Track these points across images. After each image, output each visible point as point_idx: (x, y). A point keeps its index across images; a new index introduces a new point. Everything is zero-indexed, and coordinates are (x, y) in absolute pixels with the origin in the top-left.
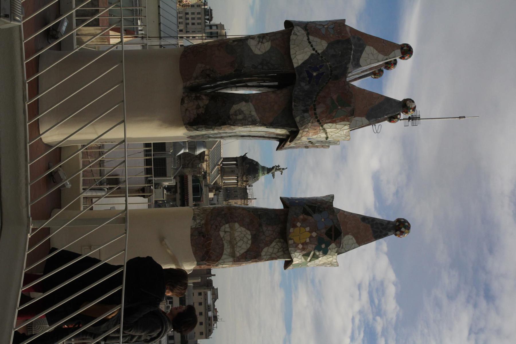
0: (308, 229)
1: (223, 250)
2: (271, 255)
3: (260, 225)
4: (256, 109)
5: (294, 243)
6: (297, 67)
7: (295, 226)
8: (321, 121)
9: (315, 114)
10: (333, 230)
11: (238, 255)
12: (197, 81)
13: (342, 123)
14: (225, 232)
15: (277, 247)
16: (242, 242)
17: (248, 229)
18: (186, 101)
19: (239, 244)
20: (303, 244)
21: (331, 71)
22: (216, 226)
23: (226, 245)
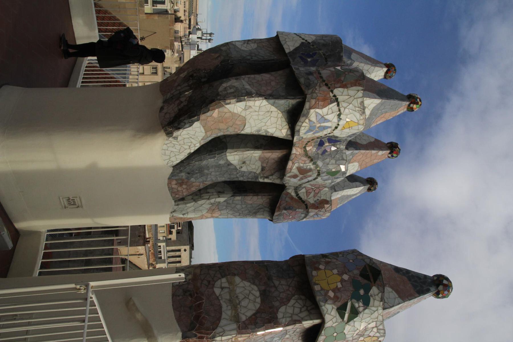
0: (335, 271)
1: (221, 313)
2: (291, 317)
3: (270, 278)
4: (250, 85)
5: (322, 289)
6: (289, 53)
7: (318, 269)
8: (329, 85)
9: (321, 77)
10: (368, 270)
11: (244, 318)
12: (179, 88)
13: (354, 88)
14: (222, 288)
15: (297, 305)
16: (247, 301)
17: (254, 283)
18: (165, 108)
19: (243, 303)
20: (333, 291)
21: (326, 59)
22: (209, 282)
23: (224, 306)
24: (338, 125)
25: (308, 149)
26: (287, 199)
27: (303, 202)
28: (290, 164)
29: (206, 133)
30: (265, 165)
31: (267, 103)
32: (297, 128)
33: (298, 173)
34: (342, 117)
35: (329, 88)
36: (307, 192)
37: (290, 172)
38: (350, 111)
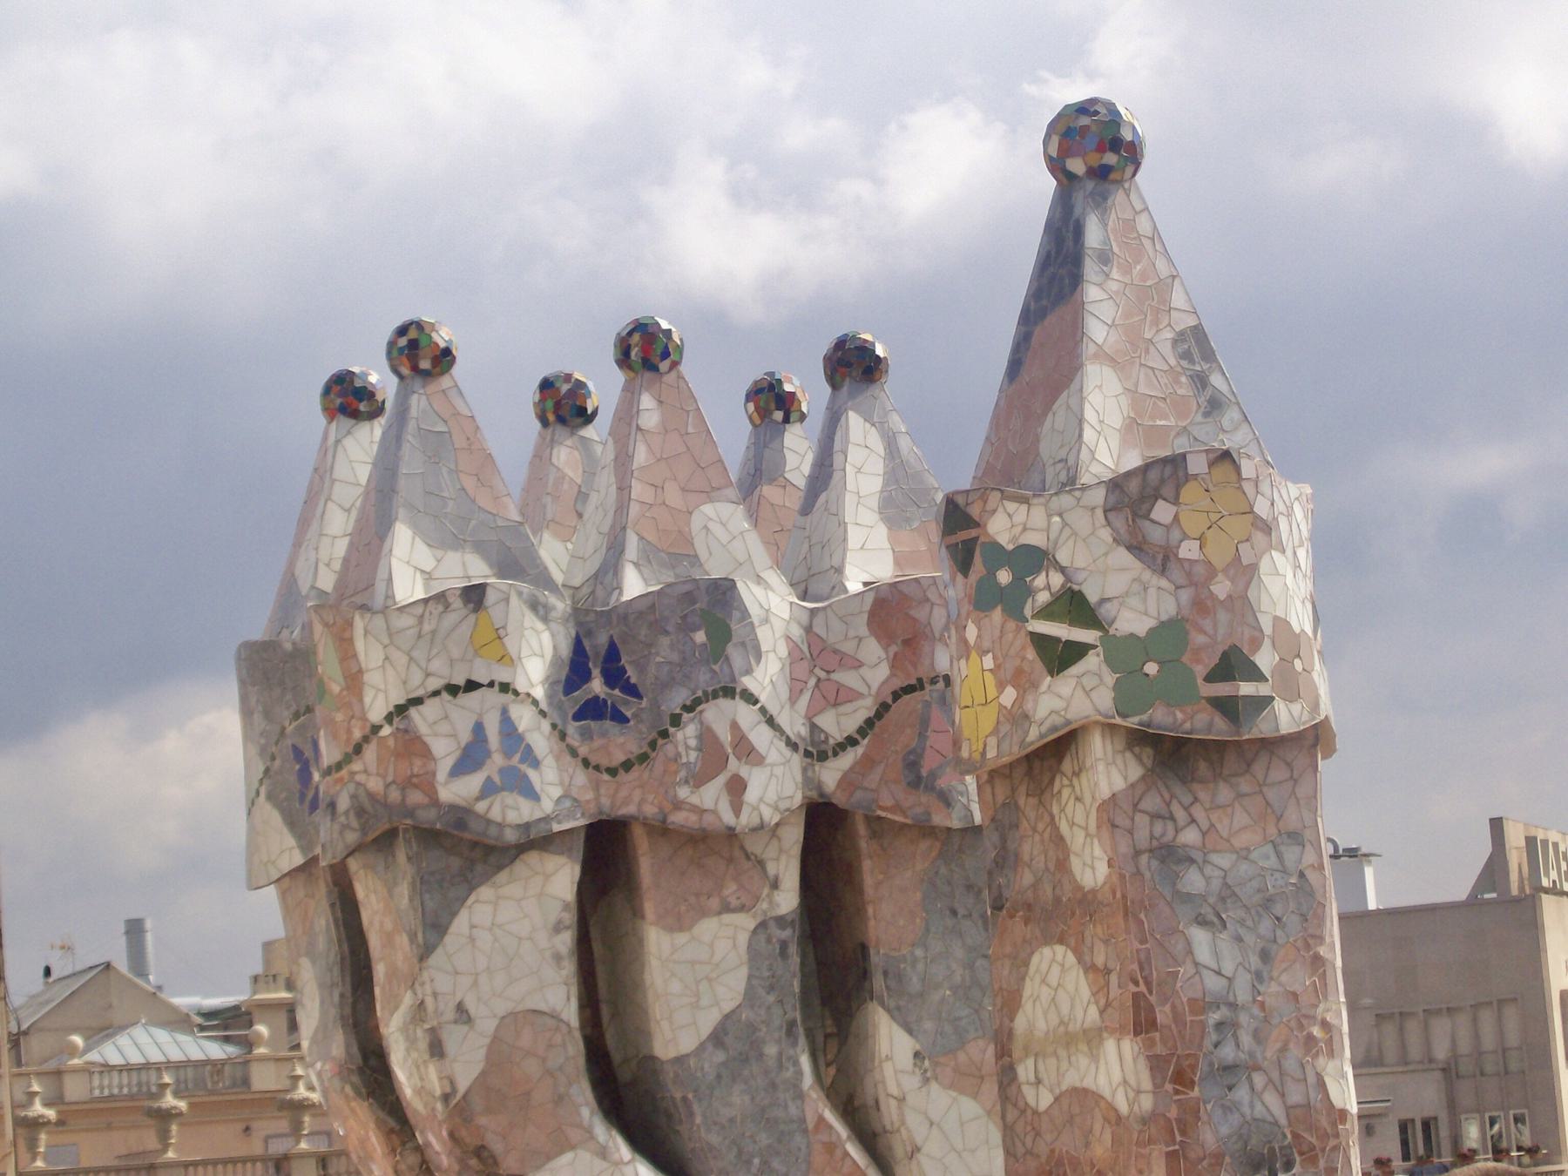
13: (360, 645)
24: (491, 684)
25: (619, 757)
26: (873, 779)
27: (883, 709)
28: (678, 818)
29: (573, 1147)
30: (714, 903)
31: (439, 950)
32: (511, 836)
33: (721, 780)
34: (461, 681)
35: (366, 739)
36: (835, 705)
37: (714, 812)
38: (435, 651)
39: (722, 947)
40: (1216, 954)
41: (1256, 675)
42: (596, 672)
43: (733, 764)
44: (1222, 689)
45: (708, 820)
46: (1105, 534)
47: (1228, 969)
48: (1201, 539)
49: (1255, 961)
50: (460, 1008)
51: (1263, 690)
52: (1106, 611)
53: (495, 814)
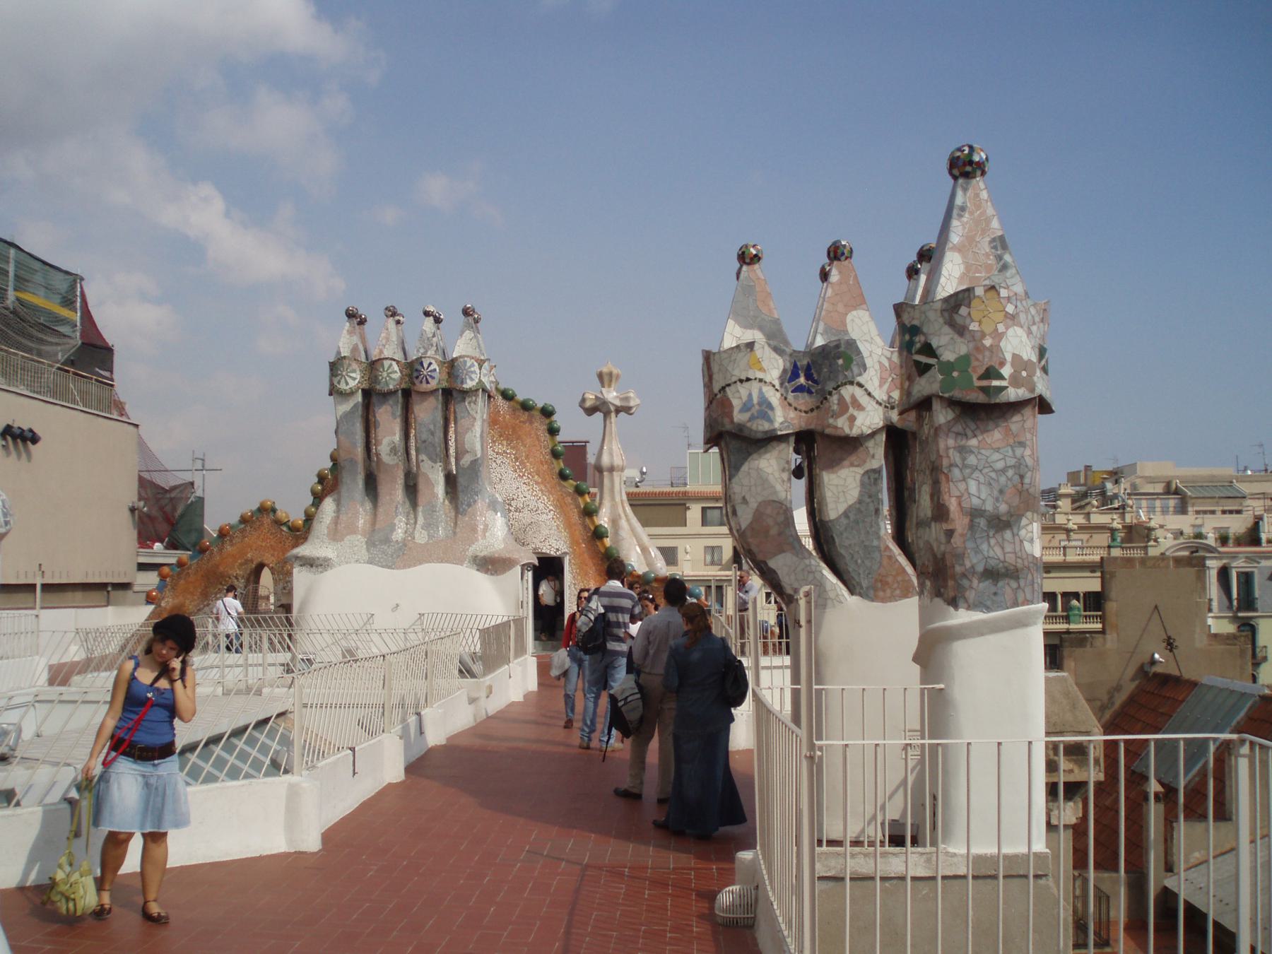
28: (828, 431)
34: (744, 378)
39: (850, 480)
40: (979, 490)
41: (1001, 377)
42: (802, 375)
43: (851, 410)
44: (984, 383)
45: (839, 433)
46: (941, 320)
47: (983, 496)
48: (980, 322)
49: (996, 493)
50: (744, 498)
51: (1004, 383)
52: (938, 352)
53: (754, 427)
